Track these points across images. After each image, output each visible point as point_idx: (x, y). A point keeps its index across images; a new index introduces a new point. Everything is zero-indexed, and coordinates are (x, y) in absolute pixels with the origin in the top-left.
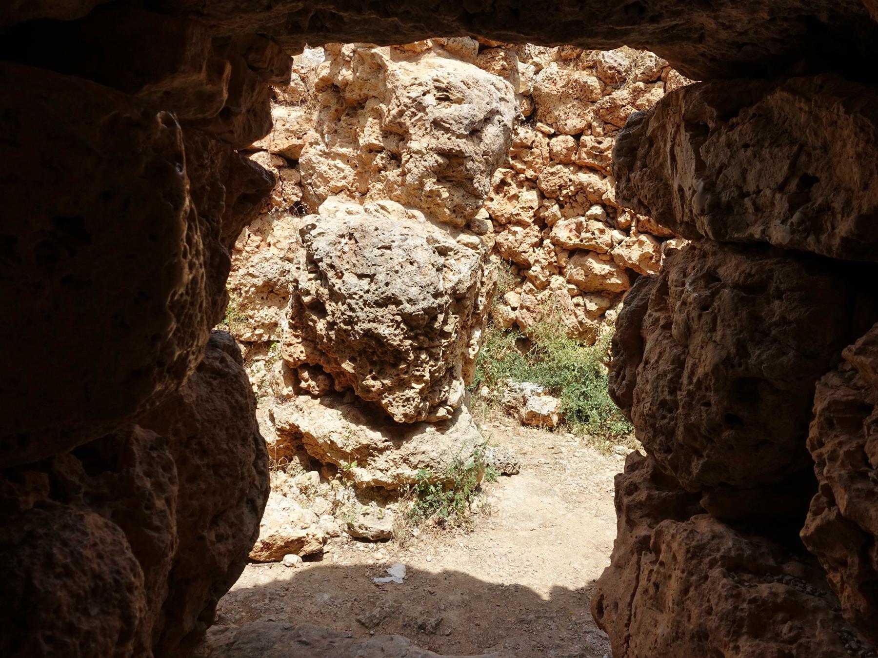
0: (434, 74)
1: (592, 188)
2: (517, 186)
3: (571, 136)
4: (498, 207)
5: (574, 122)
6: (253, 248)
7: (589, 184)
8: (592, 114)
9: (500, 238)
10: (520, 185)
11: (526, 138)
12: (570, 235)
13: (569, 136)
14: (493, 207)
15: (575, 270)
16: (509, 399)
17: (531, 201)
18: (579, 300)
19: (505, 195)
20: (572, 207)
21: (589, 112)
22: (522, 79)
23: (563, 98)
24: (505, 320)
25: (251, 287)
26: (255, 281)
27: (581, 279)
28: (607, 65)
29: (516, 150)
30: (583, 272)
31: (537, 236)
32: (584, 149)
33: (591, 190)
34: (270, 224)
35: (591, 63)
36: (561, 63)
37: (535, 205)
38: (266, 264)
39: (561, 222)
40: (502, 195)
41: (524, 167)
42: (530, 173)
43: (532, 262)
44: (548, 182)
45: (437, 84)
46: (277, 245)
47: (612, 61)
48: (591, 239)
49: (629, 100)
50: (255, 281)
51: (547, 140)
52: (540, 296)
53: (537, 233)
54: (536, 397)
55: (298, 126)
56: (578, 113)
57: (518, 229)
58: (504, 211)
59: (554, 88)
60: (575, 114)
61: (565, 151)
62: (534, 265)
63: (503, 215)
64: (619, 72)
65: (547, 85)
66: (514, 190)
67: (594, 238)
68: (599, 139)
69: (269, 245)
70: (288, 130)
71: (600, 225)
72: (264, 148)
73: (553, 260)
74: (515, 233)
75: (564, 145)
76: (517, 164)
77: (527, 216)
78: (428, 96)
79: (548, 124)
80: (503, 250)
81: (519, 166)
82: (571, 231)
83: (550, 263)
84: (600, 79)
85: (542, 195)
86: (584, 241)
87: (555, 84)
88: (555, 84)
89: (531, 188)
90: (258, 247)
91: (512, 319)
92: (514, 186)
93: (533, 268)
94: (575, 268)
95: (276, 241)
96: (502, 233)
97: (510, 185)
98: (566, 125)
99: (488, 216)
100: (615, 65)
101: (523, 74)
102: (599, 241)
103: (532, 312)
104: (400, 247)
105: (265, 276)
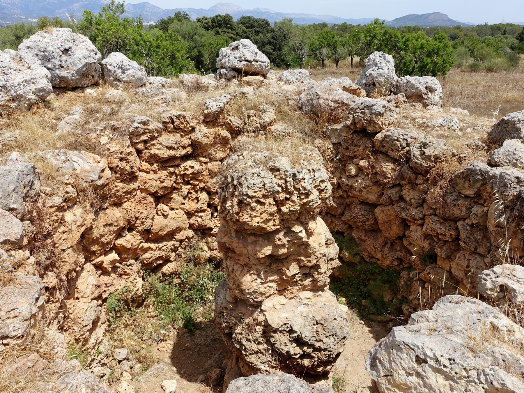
9: (193, 220)
10: (197, 192)
14: (186, 208)
19: (189, 199)
23: (213, 144)
24: (205, 259)
26: (88, 328)
37: (207, 199)
42: (202, 185)
43: (213, 227)
47: (236, 124)
55: (82, 219)
57: (202, 214)
59: (209, 140)
64: (240, 129)
66: (194, 195)
70: (79, 226)
74: (201, 217)
77: (205, 207)
79: (204, 157)
81: (198, 183)
84: (228, 131)
85: (209, 193)
92: (194, 193)
93: (214, 230)
96: (192, 218)
97: (191, 193)
100: (239, 126)
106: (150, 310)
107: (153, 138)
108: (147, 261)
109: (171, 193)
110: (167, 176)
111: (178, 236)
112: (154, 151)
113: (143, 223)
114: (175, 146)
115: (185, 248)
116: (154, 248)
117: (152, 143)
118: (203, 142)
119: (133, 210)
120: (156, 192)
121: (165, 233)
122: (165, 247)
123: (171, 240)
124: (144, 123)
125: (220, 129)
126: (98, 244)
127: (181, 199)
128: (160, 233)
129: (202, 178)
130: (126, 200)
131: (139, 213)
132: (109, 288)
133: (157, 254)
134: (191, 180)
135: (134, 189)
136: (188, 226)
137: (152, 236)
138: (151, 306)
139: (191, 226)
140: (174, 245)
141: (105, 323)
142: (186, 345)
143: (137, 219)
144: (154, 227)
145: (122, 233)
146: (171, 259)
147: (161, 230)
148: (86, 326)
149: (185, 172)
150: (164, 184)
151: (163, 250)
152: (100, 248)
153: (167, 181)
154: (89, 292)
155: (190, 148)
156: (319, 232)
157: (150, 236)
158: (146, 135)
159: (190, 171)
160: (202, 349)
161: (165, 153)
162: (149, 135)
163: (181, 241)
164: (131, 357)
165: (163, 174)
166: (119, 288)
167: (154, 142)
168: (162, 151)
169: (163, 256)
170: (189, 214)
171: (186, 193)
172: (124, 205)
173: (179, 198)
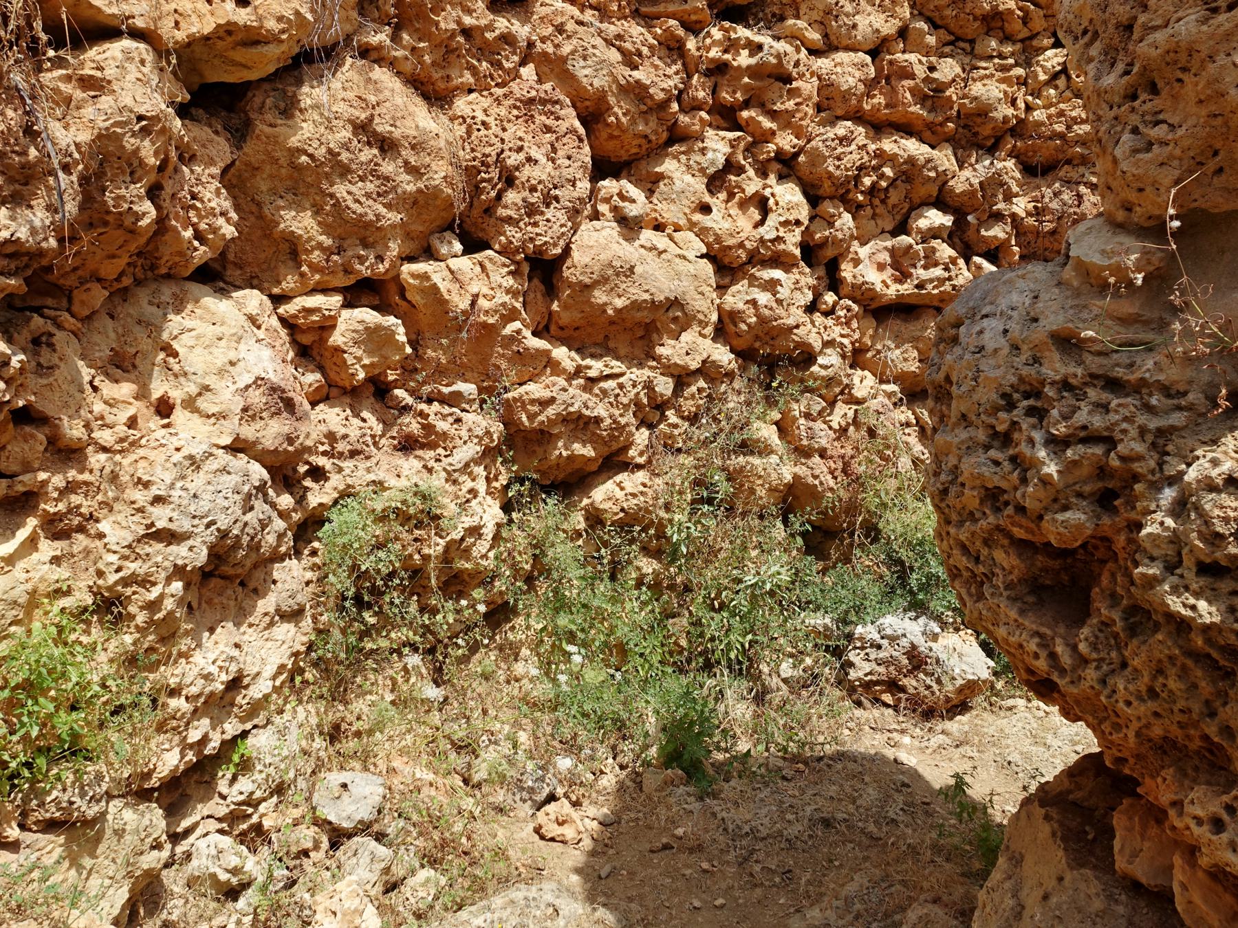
1: (935, 168)
2: (757, 171)
3: (866, 53)
4: (726, 225)
6: (122, 430)
7: (929, 161)
9: (737, 297)
10: (763, 173)
13: (861, 54)
15: (898, 352)
16: (867, 667)
19: (731, 196)
20: (874, 217)
24: (772, 490)
25: (168, 580)
26: (180, 553)
27: (913, 369)
29: (758, 84)
30: (916, 354)
32: (908, 83)
33: (933, 174)
34: (153, 328)
38: (197, 481)
40: (723, 196)
41: (773, 126)
42: (786, 141)
43: (817, 345)
44: (839, 159)
46: (202, 403)
48: (942, 281)
50: (180, 553)
57: (777, 274)
61: (861, 87)
62: (821, 352)
63: (741, 245)
66: (752, 184)
67: (950, 279)
69: (164, 408)
72: (140, 23)
74: (771, 286)
76: (761, 118)
77: (792, 242)
80: (744, 327)
81: (767, 124)
86: (930, 287)
89: (781, 178)
90: (132, 423)
94: (897, 347)
95: (193, 389)
96: (734, 289)
97: (740, 170)
98: (855, 26)
99: (704, 250)
105: (208, 526)
106: (519, 668)
108: (531, 417)
109: (658, 151)
110: (651, 47)
111: (669, 350)
113: (532, 210)
115: (693, 419)
116: (569, 365)
119: (494, 129)
120: (601, 96)
121: (620, 303)
122: (610, 384)
123: (641, 365)
126: (317, 210)
127: (699, 184)
128: (600, 296)
129: (790, 105)
130: (468, 78)
131: (522, 156)
132: (348, 465)
133: (577, 399)
134: (746, 105)
135: (507, 39)
136: (714, 317)
137: (565, 307)
138: (525, 652)
139: (721, 332)
140: (649, 386)
141: (294, 615)
142: (680, 832)
143: (509, 181)
144: (576, 255)
145: (435, 242)
146: (632, 453)
147: (604, 280)
148: (170, 537)
149: (728, 57)
151: (604, 392)
152: (327, 241)
154: (226, 397)
157: (555, 306)
159: (744, 59)
160: (761, 856)
163: (682, 378)
164: (393, 827)
166: (392, 481)
169: (598, 420)
171: (721, 160)
172: (462, 105)
173: (688, 178)
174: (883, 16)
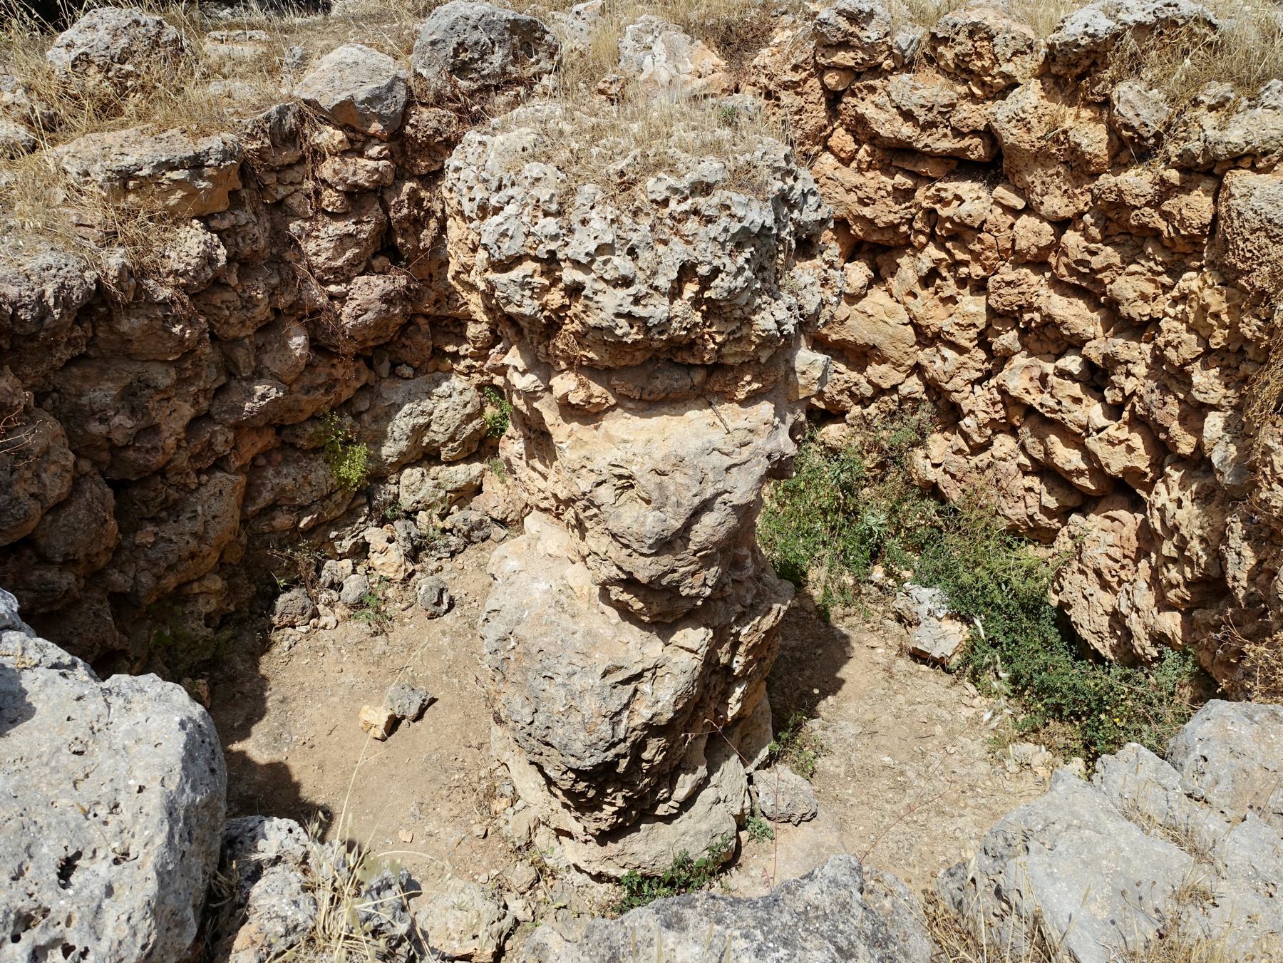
0: (616, 455)
4: (922, 311)
5: (1056, 203)
7: (1063, 323)
8: (1088, 197)
10: (962, 283)
11: (970, 216)
12: (1029, 385)
17: (974, 315)
18: (1033, 481)
19: (936, 293)
21: (1082, 194)
22: (802, 381)
23: (1041, 157)
28: (1120, 120)
31: (980, 370)
35: (1100, 99)
36: (1049, 82)
37: (981, 321)
39: (1020, 360)
40: (932, 290)
41: (967, 257)
42: (977, 270)
43: (965, 410)
45: (617, 471)
47: (1130, 114)
49: (1149, 198)
51: (1010, 219)
52: (975, 460)
53: (979, 366)
54: (933, 620)
56: (1064, 188)
57: (948, 353)
58: (931, 321)
59: (1026, 137)
60: (1060, 188)
63: (928, 327)
65: (1015, 131)
66: (950, 288)
68: (1093, 246)
71: (1076, 390)
73: (997, 416)
75: (1034, 239)
78: (602, 489)
81: (960, 256)
82: (1031, 379)
83: (993, 420)
87: (1029, 130)
88: (1029, 130)
91: (930, 481)
92: (951, 282)
100: (1136, 124)
101: (804, 373)
102: (1067, 417)
103: (960, 481)
104: (564, 685)
107: (877, 71)
111: (874, 370)
112: (866, 108)
114: (922, 116)
117: (871, 82)
118: (1004, 134)
124: (852, 18)
125: (1086, 114)
134: (950, 238)
149: (938, 206)
150: (867, 212)
153: (879, 206)
155: (977, 141)
156: (612, 432)
158: (852, 54)
161: (889, 126)
162: (860, 54)
165: (875, 180)
167: (877, 83)
168: (882, 116)
170: (926, 337)
174: (1066, 201)
